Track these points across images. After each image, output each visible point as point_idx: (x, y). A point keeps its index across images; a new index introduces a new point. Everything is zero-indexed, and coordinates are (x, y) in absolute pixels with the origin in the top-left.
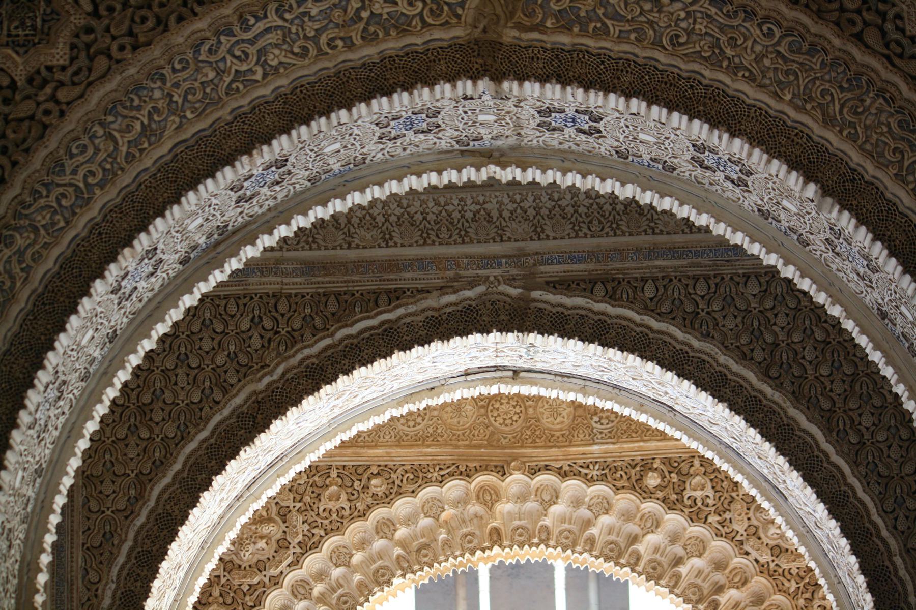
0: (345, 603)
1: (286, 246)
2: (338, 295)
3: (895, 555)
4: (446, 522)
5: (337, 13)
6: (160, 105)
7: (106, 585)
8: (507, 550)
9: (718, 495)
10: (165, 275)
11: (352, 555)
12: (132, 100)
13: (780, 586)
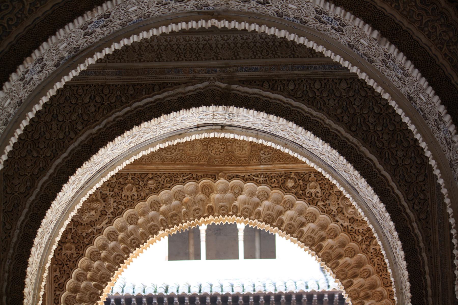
0: (134, 243)
1: (108, 60)
2: (134, 85)
3: (413, 222)
4: (186, 203)
7: (14, 231)
8: (216, 217)
9: (323, 192)
10: (47, 72)
11: (138, 219)
13: (354, 238)
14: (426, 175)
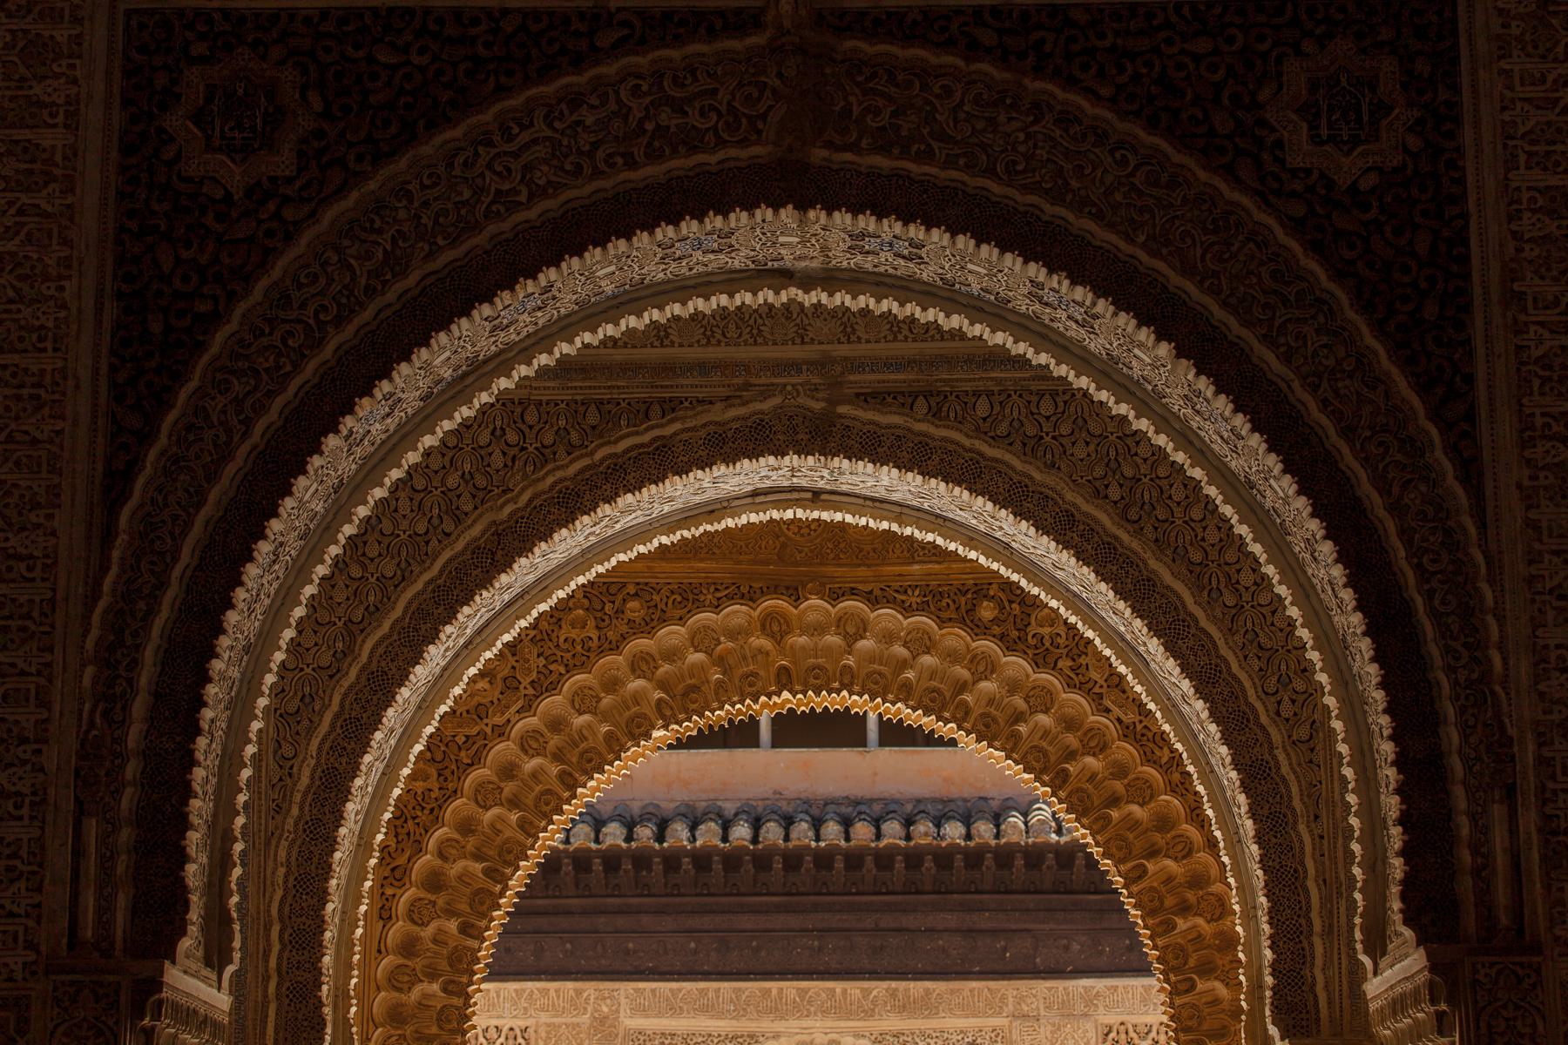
0: (590, 761)
7: (303, 762)
8: (800, 696)
10: (403, 414)
11: (599, 700)
12: (372, 221)
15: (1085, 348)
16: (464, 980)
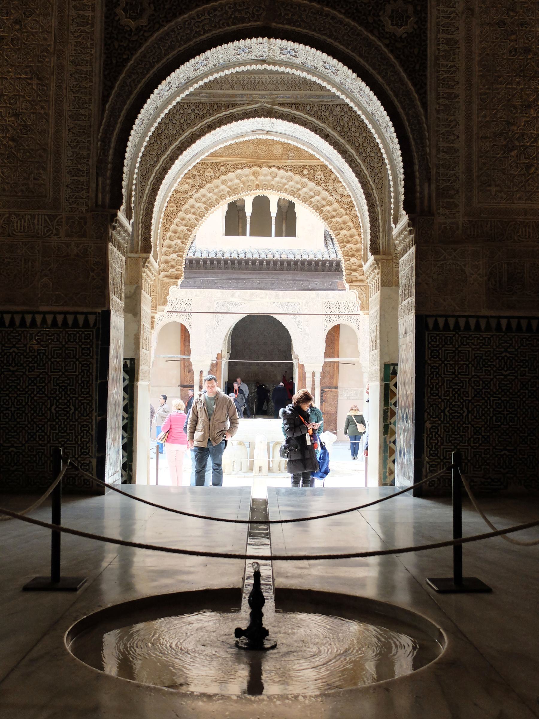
2: (217, 104)
5: (225, 16)
6: (174, 39)
14: (383, 163)
15: (335, 81)
16: (182, 254)
